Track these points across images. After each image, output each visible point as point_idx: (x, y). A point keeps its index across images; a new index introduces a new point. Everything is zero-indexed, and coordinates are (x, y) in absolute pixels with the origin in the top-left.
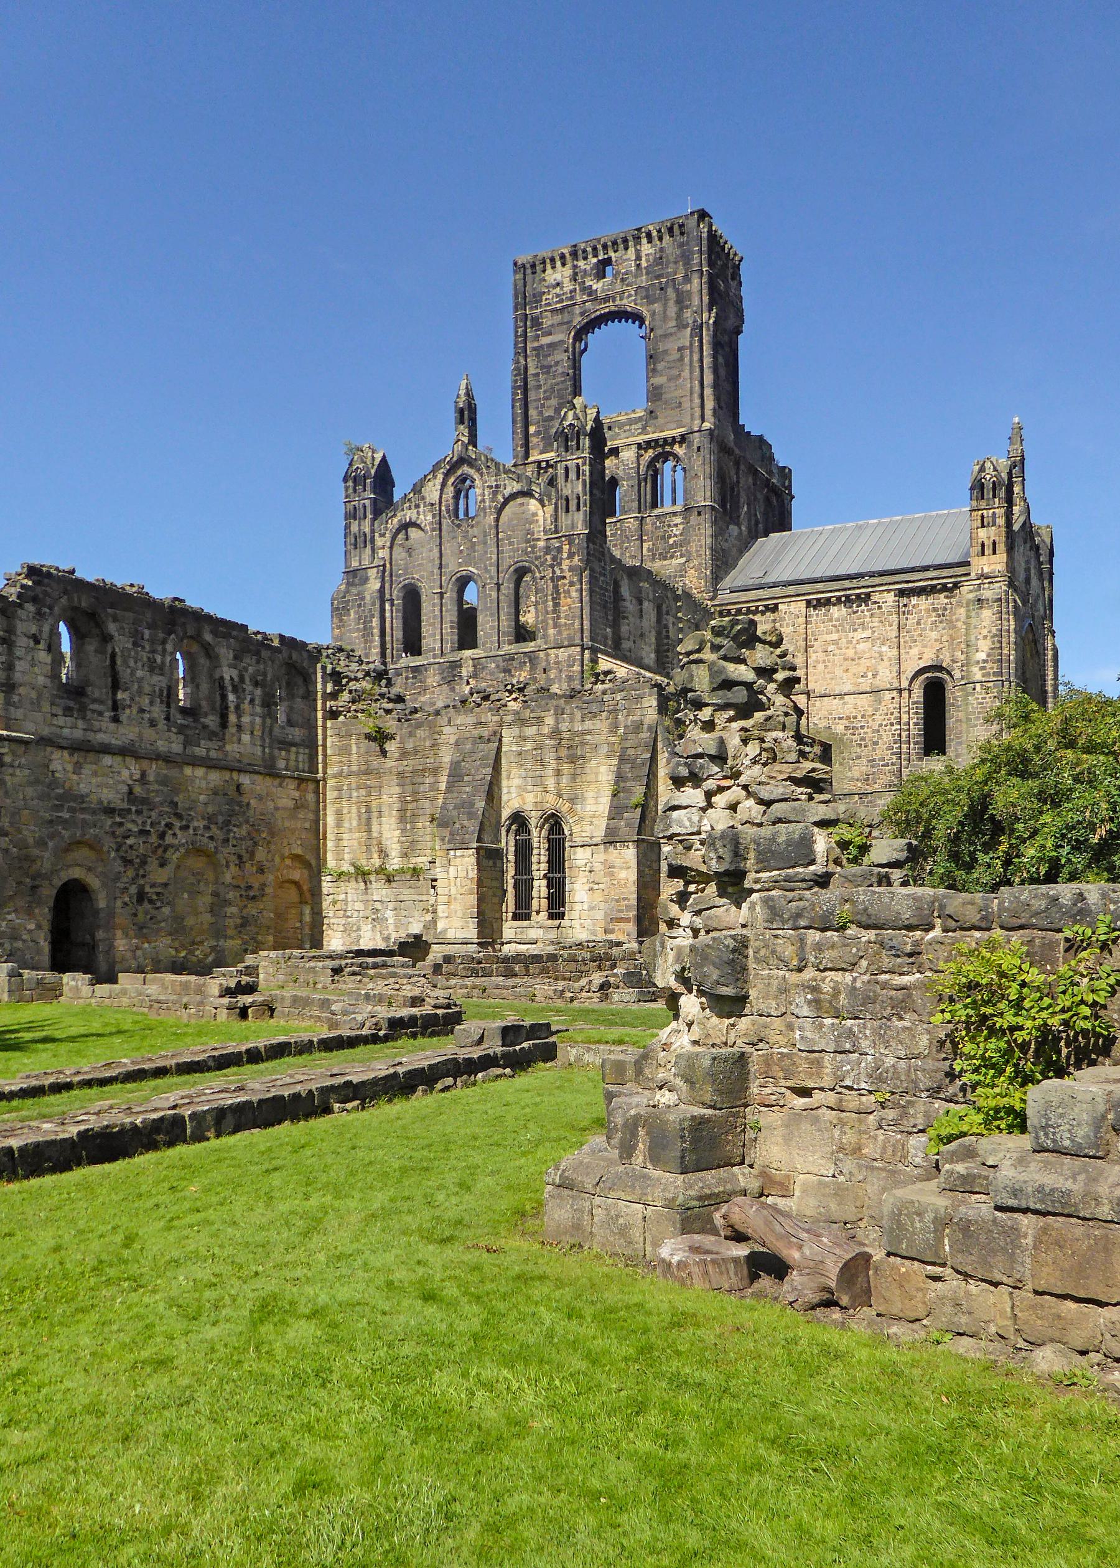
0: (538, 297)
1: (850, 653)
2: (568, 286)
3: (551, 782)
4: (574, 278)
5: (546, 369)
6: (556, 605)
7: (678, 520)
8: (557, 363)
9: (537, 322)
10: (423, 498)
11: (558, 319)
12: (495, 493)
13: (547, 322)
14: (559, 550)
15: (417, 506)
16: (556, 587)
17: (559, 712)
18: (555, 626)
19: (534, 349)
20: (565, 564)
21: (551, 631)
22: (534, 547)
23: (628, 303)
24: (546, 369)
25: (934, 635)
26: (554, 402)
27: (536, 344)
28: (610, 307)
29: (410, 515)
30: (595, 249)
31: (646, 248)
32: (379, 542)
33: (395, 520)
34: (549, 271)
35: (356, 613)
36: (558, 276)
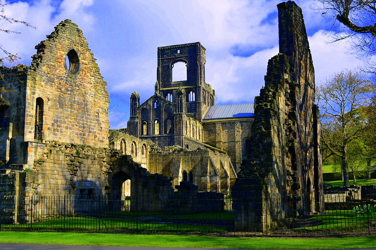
1: (231, 134)
3: (191, 166)
6: (176, 127)
7: (194, 104)
11: (168, 60)
12: (163, 104)
14: (177, 116)
15: (146, 105)
16: (176, 123)
17: (192, 154)
18: (176, 131)
20: (178, 119)
21: (175, 132)
22: (171, 115)
25: (248, 130)
29: (145, 107)
31: (187, 48)
34: (166, 50)
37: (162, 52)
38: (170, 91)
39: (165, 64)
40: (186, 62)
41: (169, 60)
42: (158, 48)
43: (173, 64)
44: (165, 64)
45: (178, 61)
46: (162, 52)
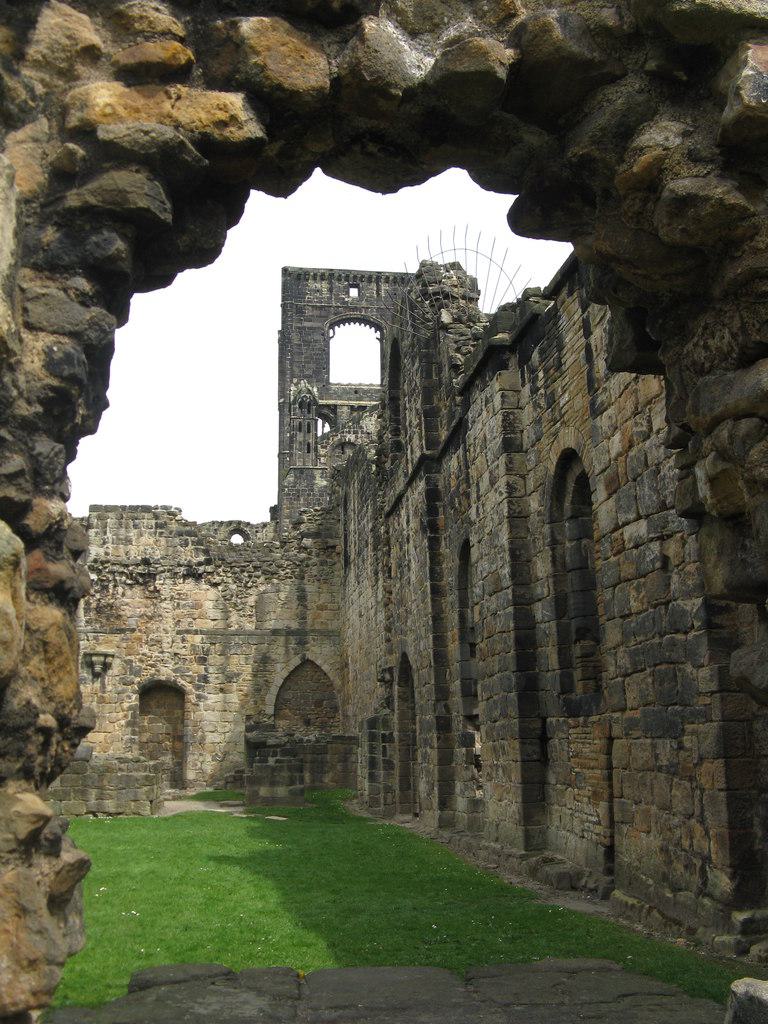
0: (301, 295)
2: (326, 294)
4: (330, 290)
5: (308, 343)
8: (316, 341)
9: (300, 311)
10: (361, 428)
11: (316, 313)
13: (308, 312)
19: (299, 328)
23: (373, 315)
24: (308, 343)
26: (312, 366)
27: (299, 325)
28: (357, 314)
30: (348, 276)
31: (384, 287)
32: (322, 452)
33: (336, 439)
35: (305, 500)
36: (318, 286)
37: (294, 281)
38: (325, 411)
39: (307, 324)
40: (378, 327)
41: (323, 313)
42: (285, 271)
43: (332, 326)
44: (307, 324)
45: (349, 320)
46: (294, 281)
